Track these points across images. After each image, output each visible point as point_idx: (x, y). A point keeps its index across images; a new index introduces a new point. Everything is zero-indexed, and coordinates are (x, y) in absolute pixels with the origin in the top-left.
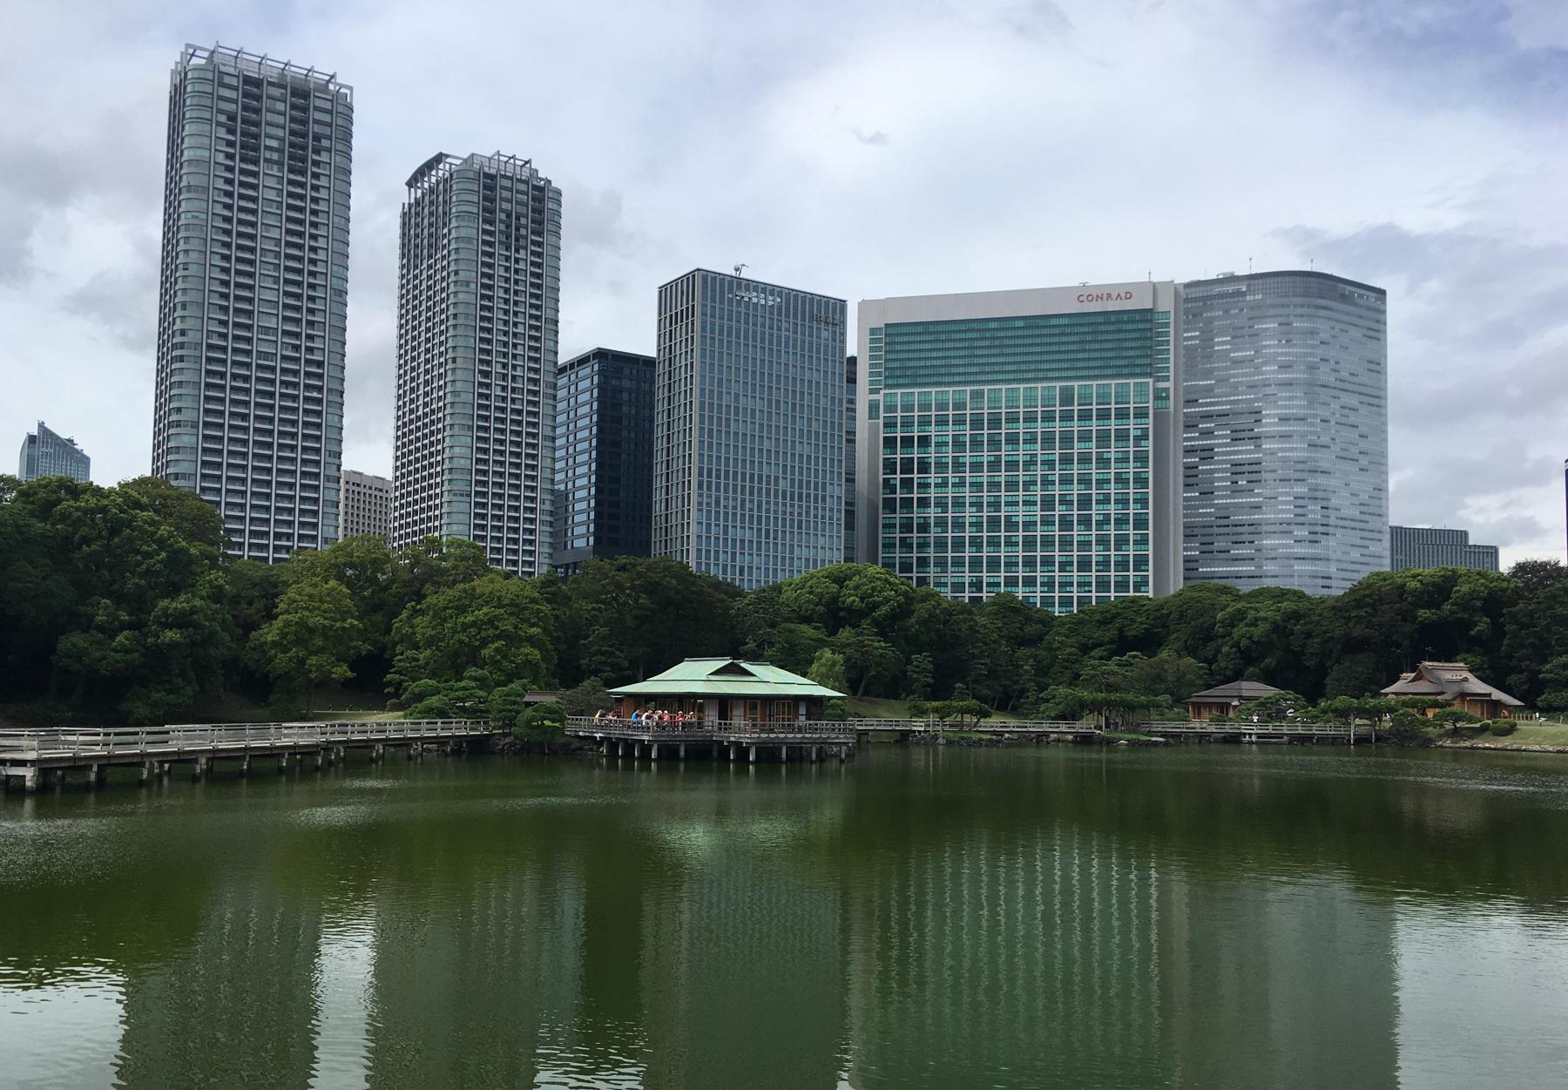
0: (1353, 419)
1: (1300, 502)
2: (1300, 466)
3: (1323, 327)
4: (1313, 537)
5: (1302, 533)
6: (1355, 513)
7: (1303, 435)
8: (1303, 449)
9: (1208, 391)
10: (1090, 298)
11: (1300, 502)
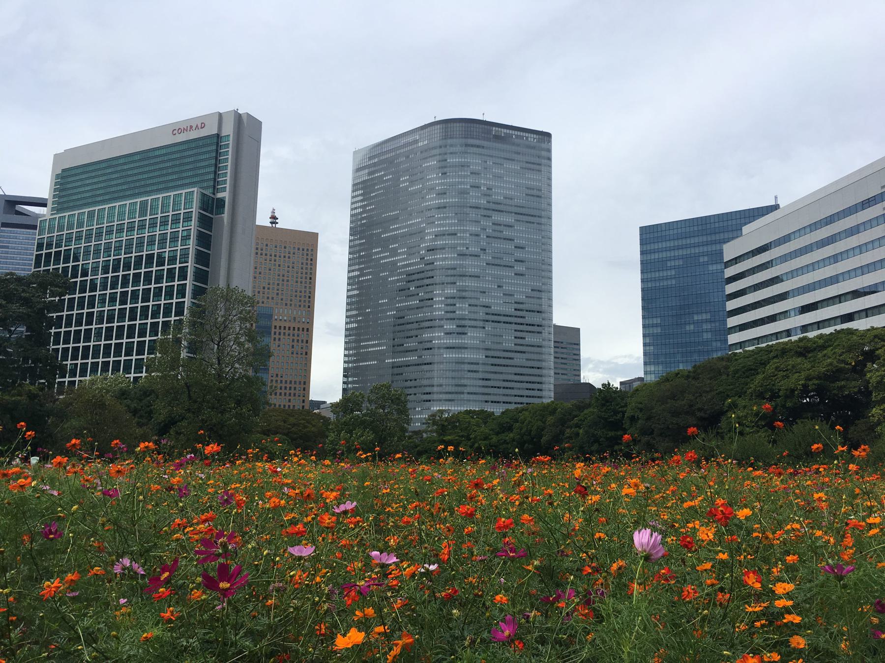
0: (507, 233)
1: (450, 301)
2: (450, 272)
3: (475, 162)
4: (460, 330)
5: (450, 326)
6: (510, 310)
7: (453, 247)
8: (452, 259)
9: (395, 219)
10: (181, 131)
11: (450, 301)
